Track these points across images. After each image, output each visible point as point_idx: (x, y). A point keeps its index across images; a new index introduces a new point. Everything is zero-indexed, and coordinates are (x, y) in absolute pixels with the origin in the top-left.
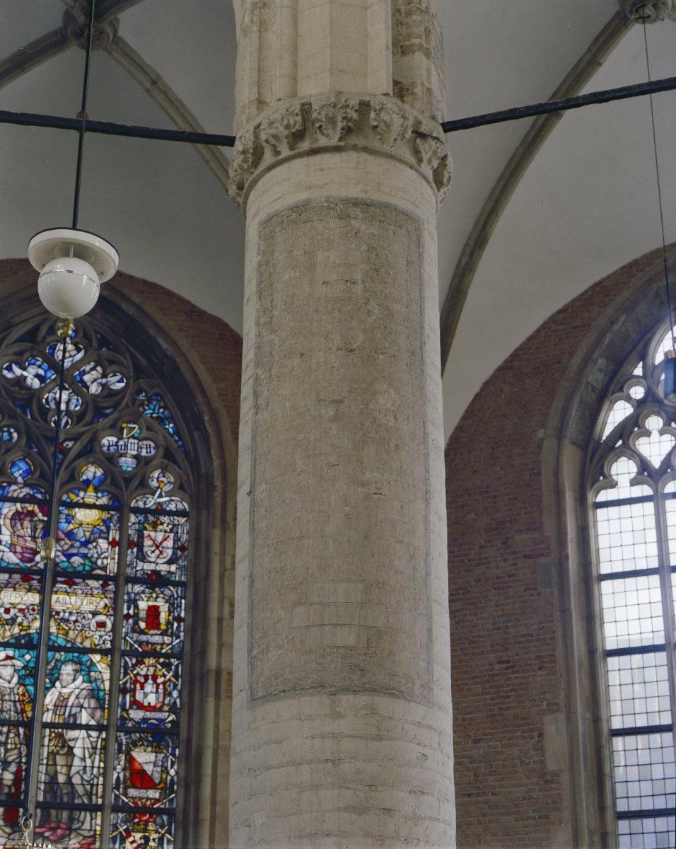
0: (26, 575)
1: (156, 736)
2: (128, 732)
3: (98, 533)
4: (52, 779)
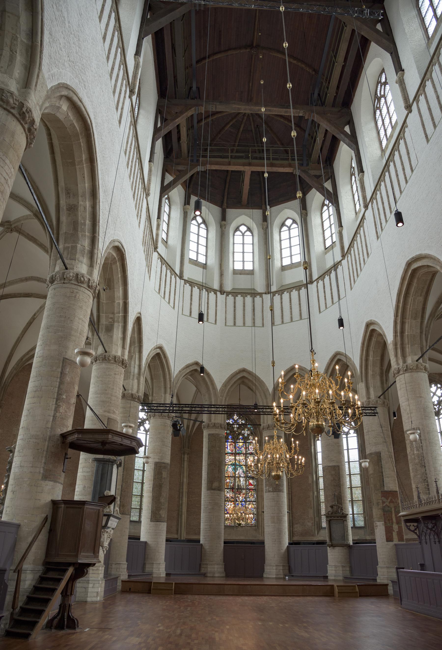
0: (232, 454)
1: (252, 478)
2: (248, 477)
3: (242, 447)
4: (238, 485)
